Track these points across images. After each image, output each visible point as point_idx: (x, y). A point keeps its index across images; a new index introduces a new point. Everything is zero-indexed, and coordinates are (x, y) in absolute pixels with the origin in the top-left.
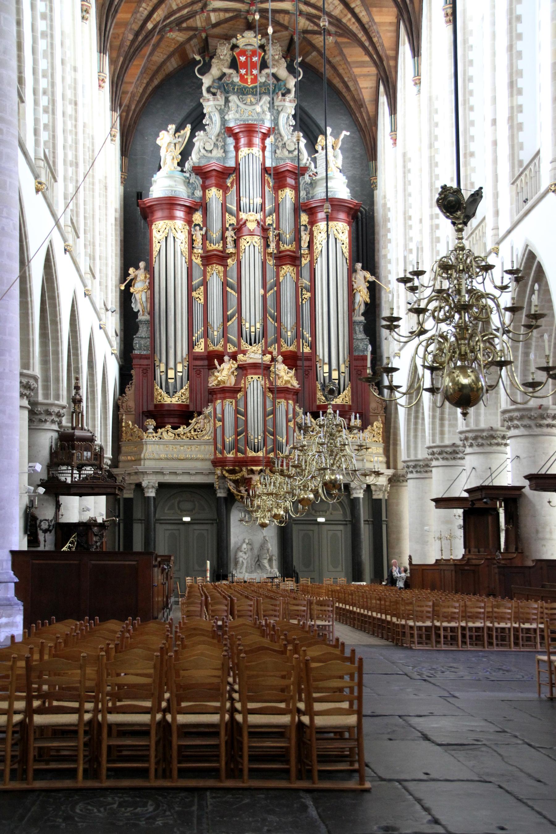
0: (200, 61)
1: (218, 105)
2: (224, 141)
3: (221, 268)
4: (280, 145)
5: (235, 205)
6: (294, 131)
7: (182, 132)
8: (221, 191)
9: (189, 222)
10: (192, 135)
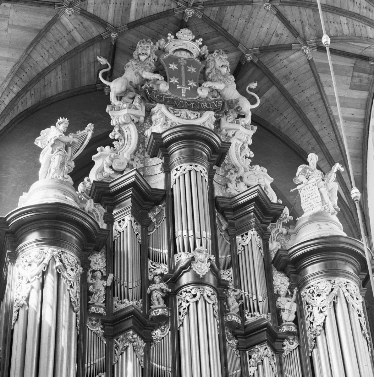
3: (141, 343)
4: (233, 177)
5: (166, 246)
7: (79, 133)
8: (139, 226)
9: (85, 263)
10: (92, 149)
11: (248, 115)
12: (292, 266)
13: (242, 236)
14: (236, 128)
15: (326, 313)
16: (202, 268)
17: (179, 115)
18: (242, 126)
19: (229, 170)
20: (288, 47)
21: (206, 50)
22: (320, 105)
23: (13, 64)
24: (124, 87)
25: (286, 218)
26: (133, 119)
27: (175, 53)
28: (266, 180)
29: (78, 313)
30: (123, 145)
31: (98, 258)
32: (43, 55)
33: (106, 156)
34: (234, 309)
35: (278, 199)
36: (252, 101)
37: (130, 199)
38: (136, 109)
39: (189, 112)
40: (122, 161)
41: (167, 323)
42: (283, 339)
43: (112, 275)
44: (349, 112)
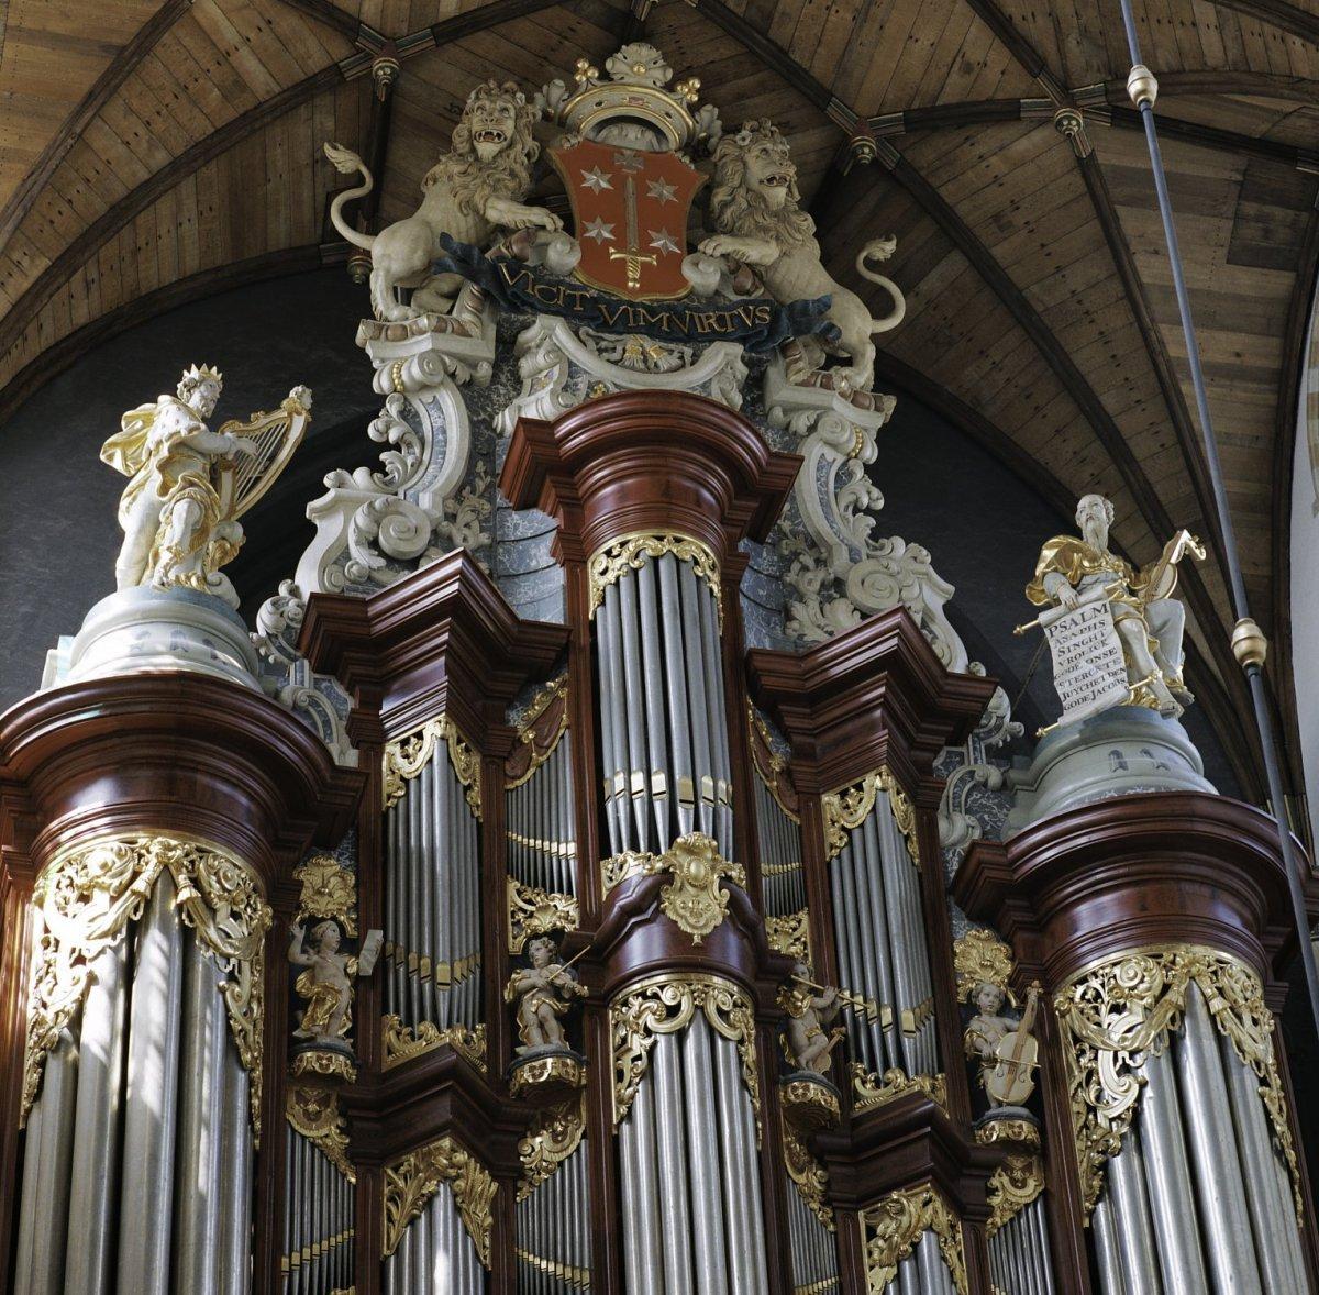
0: (358, 180)
1: (462, 359)
2: (490, 523)
4: (811, 582)
6: (875, 535)
7: (260, 421)
8: (476, 759)
9: (280, 891)
10: (303, 479)
11: (863, 355)
12: (1022, 903)
13: (844, 794)
14: (819, 403)
15: (1144, 1073)
16: (700, 910)
17: (616, 356)
18: (842, 395)
19: (796, 555)
20: (1006, 112)
21: (712, 122)
22: (1117, 319)
23: (22, 169)
24: (420, 252)
25: (998, 727)
26: (451, 370)
27: (604, 132)
28: (927, 592)
29: (258, 1073)
30: (418, 463)
31: (328, 871)
32: (130, 138)
33: (358, 502)
34: (814, 1060)
35: (971, 659)
36: (879, 305)
37: (442, 659)
38: (465, 334)
39: (652, 348)
40: (413, 521)
41: (574, 1109)
42: (990, 1169)
43: (379, 934)
44: (1224, 346)
